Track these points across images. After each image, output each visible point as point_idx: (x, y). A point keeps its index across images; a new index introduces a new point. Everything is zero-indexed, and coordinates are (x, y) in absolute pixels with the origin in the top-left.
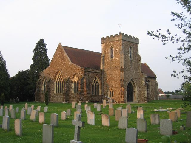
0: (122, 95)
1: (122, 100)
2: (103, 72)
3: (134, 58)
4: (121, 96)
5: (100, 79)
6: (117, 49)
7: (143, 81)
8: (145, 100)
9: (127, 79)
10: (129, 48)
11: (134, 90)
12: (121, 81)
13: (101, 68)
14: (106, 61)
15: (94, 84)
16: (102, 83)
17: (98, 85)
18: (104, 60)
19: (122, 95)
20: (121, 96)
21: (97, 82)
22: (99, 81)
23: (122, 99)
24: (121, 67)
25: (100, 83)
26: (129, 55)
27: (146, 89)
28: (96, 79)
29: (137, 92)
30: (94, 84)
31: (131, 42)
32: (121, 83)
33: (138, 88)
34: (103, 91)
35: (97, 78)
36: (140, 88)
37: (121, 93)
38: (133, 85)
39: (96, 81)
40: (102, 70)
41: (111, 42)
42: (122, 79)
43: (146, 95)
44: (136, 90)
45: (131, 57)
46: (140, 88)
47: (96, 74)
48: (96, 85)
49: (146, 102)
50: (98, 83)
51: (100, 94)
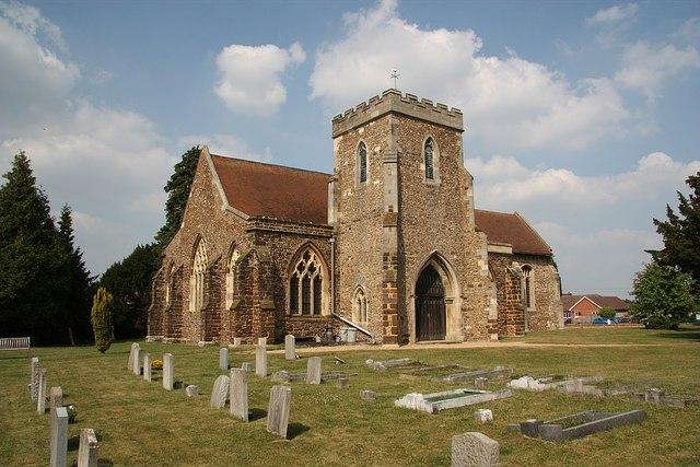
0: (389, 312)
1: (389, 334)
2: (336, 234)
3: (442, 178)
4: (385, 318)
5: (326, 258)
6: (377, 149)
7: (481, 263)
8: (491, 332)
9: (414, 255)
10: (420, 144)
11: (447, 296)
12: (385, 259)
13: (331, 220)
14: (347, 193)
15: (301, 277)
16: (330, 274)
17: (318, 281)
18: (337, 193)
19: (389, 312)
20: (385, 318)
21: (312, 269)
22: (317, 266)
23: (389, 329)
24: (387, 210)
25: (322, 274)
26: (423, 167)
27: (494, 291)
28: (307, 257)
29: (458, 303)
30: (301, 277)
31: (432, 123)
32: (385, 268)
33: (462, 286)
34: (336, 303)
35: (312, 254)
36: (472, 286)
37: (385, 306)
38: (444, 278)
39: (309, 263)
40: (332, 228)
41: (360, 126)
42: (388, 254)
43: (493, 313)
44: (454, 291)
45: (430, 175)
46: (472, 286)
47: (307, 240)
48: (306, 280)
49: (495, 336)
50: (315, 274)
51: (325, 312)
